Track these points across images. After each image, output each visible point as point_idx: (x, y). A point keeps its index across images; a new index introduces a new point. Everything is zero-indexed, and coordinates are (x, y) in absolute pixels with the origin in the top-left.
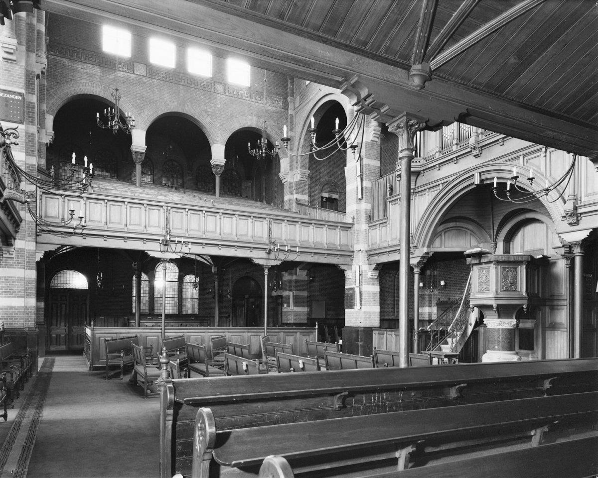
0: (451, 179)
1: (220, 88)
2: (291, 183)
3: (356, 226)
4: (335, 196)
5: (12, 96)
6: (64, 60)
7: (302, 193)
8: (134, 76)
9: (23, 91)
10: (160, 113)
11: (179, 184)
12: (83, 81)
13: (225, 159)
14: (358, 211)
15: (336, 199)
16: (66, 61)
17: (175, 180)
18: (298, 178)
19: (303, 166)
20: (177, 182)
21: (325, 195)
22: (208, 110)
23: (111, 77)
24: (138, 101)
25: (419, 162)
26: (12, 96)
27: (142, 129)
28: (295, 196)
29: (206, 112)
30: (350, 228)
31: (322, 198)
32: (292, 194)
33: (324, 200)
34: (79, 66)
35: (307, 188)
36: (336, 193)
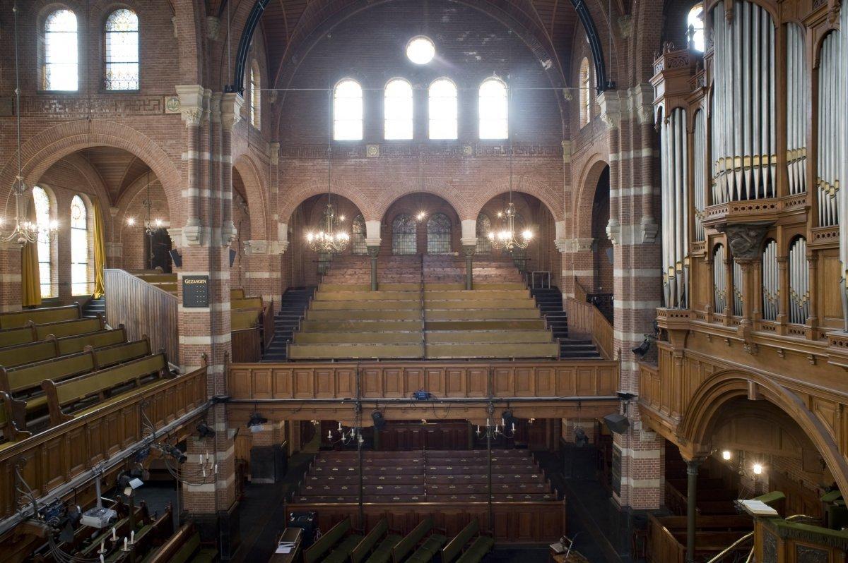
0: (725, 368)
1: (468, 150)
2: (569, 255)
3: (624, 365)
5: (198, 281)
6: (294, 161)
7: (585, 267)
8: (366, 160)
9: (207, 273)
10: (396, 196)
12: (314, 179)
14: (627, 343)
16: (297, 163)
18: (577, 248)
19: (582, 234)
22: (454, 180)
23: (343, 167)
24: (371, 188)
25: (772, 207)
26: (198, 281)
27: (376, 219)
28: (575, 273)
29: (452, 182)
30: (615, 366)
34: (309, 164)
35: (591, 260)
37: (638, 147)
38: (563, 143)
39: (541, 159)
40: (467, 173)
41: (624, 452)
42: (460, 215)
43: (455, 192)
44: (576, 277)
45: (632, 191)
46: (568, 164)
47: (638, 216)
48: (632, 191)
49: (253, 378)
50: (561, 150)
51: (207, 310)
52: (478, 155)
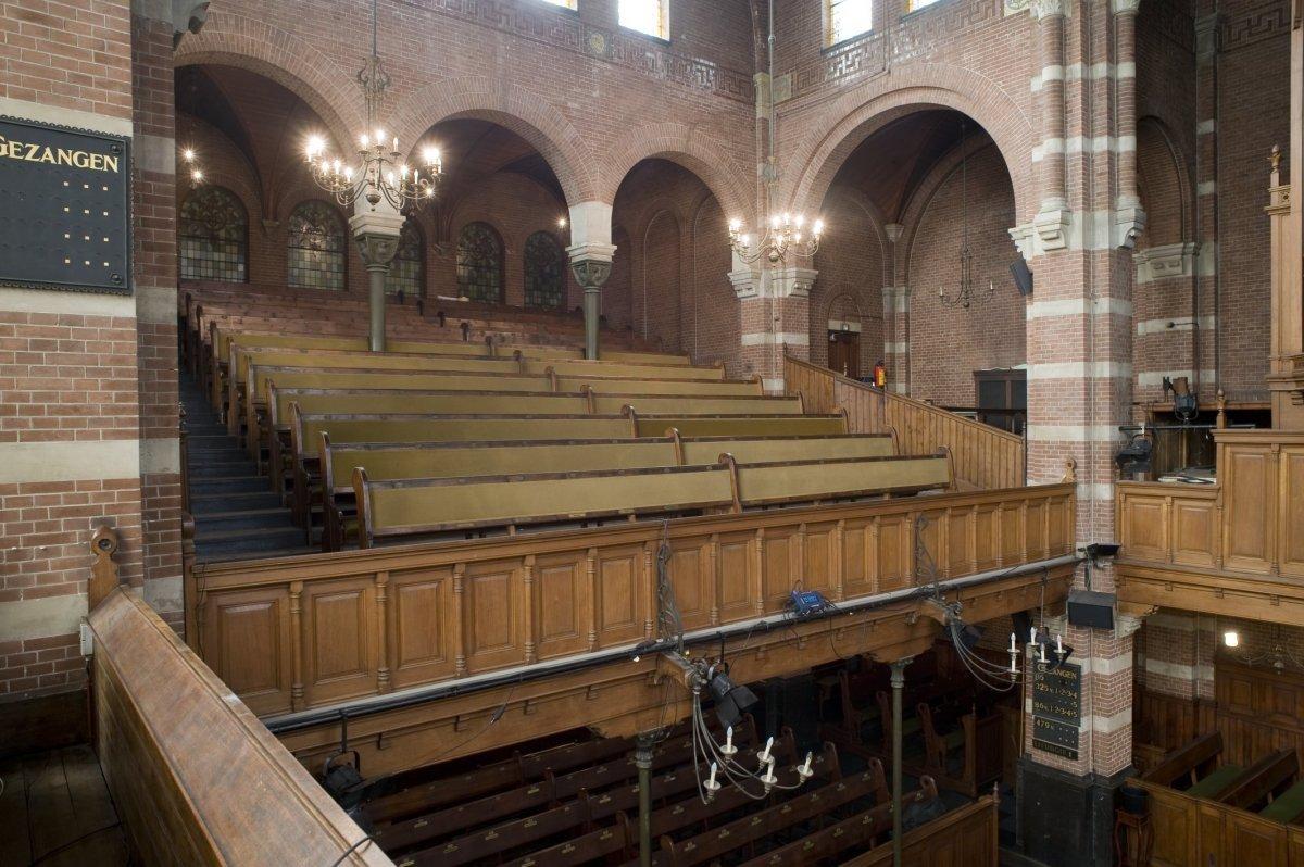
3: (1082, 491)
4: (854, 327)
5: (72, 159)
9: (124, 128)
11: (413, 275)
13: (613, 243)
15: (856, 334)
17: (402, 266)
20: (408, 271)
21: (835, 325)
22: (570, 104)
26: (72, 159)
28: (780, 338)
29: (565, 108)
31: (830, 332)
32: (769, 330)
33: (833, 337)
35: (805, 315)
36: (855, 317)
37: (1113, 60)
38: (758, 78)
39: (721, 99)
40: (596, 94)
41: (1086, 666)
42: (569, 187)
43: (570, 132)
44: (786, 347)
45: (1101, 144)
46: (765, 121)
47: (1113, 192)
48: (1101, 144)
49: (308, 619)
50: (753, 92)
51: (125, 308)
52: (616, 60)
